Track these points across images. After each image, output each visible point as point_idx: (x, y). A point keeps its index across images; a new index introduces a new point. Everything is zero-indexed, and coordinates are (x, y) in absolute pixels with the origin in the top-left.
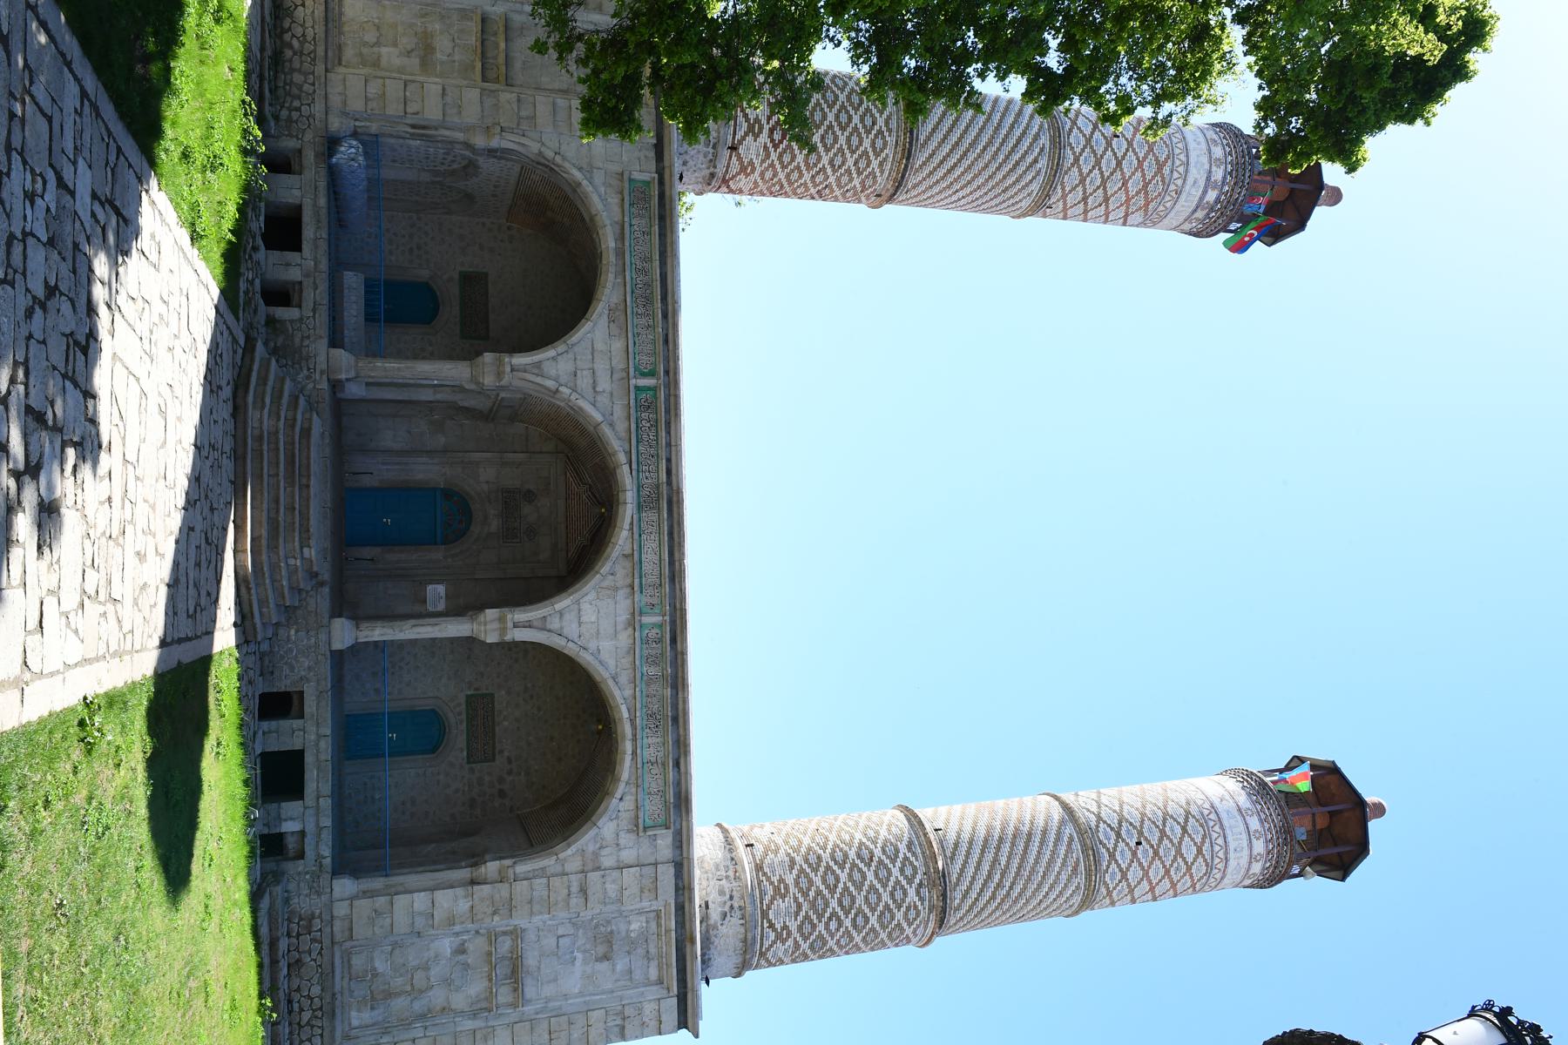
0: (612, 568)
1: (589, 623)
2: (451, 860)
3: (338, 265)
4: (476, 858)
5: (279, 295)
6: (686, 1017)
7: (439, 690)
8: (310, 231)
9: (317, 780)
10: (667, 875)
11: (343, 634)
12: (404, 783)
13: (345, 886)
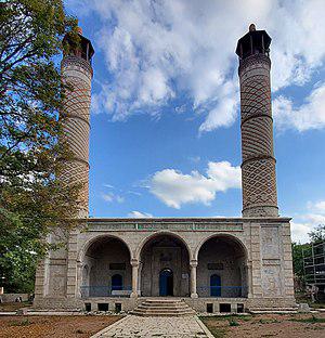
0: (181, 235)
1: (194, 242)
2: (246, 273)
3: (110, 295)
4: (246, 268)
5: (118, 307)
6: (287, 221)
7: (208, 274)
8: (104, 302)
9: (226, 301)
10: (253, 224)
11: (194, 295)
12: (226, 284)
13: (250, 295)
